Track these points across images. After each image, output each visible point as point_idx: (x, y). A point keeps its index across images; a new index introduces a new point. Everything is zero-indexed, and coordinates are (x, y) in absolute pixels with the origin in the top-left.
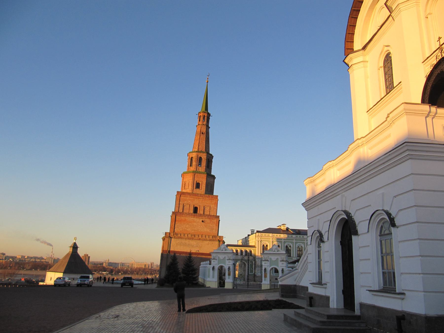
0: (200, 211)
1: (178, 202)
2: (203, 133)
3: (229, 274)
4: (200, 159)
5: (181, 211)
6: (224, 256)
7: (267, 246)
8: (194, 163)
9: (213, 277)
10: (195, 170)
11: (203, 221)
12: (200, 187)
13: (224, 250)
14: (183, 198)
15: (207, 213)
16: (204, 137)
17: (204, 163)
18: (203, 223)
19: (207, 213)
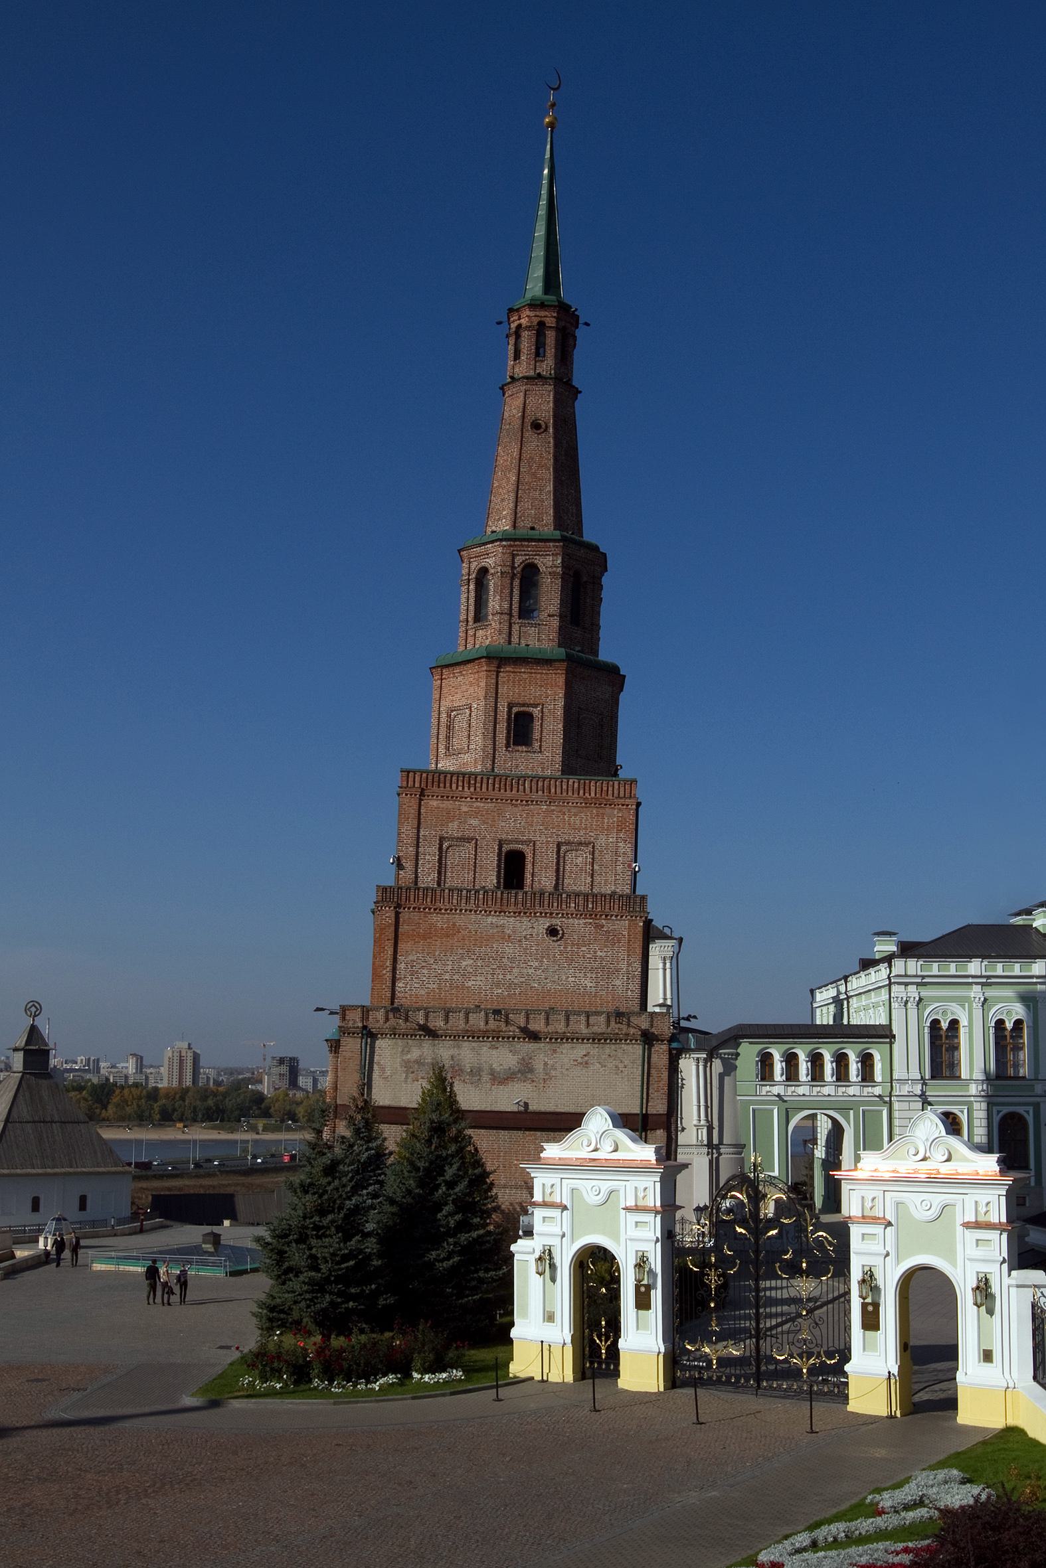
0: (540, 877)
1: (408, 830)
2: (536, 426)
3: (643, 1303)
4: (528, 578)
5: (428, 879)
6: (605, 1186)
7: (954, 1023)
8: (494, 603)
9: (550, 1317)
10: (501, 640)
11: (552, 932)
12: (536, 735)
13: (607, 1146)
14: (435, 803)
15: (576, 882)
16: (542, 448)
17: (550, 598)
18: (549, 940)
19: (576, 882)
